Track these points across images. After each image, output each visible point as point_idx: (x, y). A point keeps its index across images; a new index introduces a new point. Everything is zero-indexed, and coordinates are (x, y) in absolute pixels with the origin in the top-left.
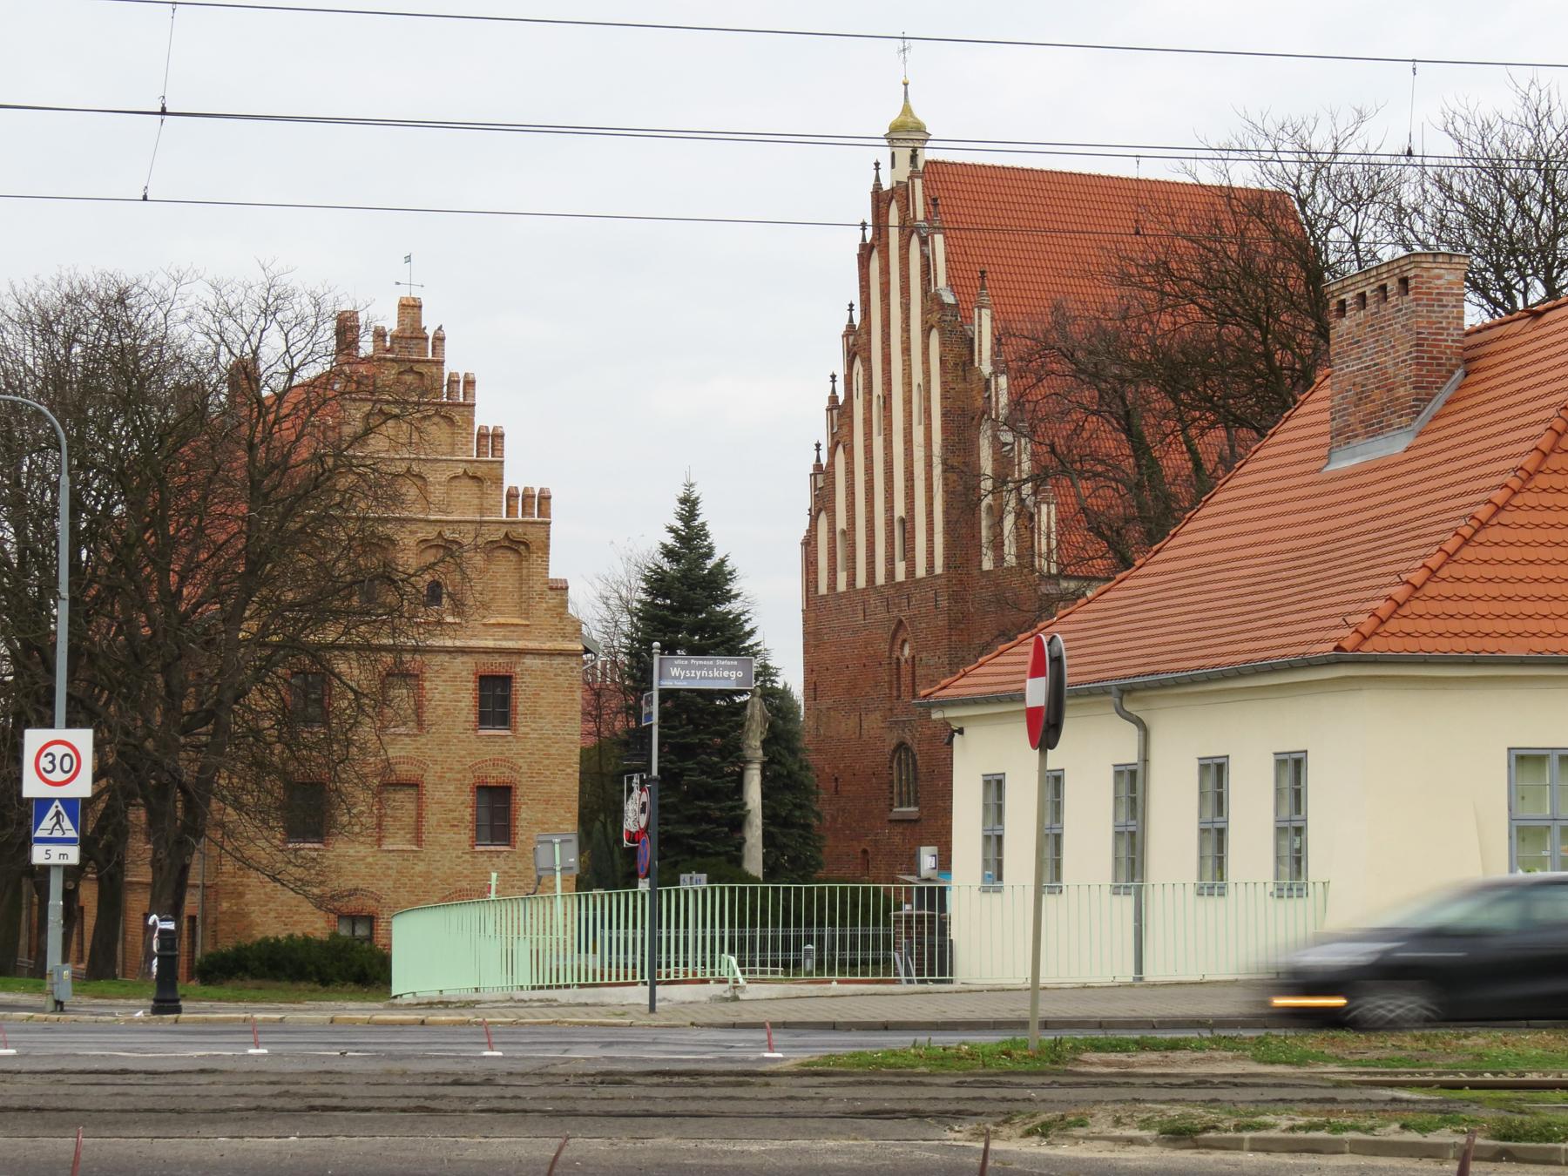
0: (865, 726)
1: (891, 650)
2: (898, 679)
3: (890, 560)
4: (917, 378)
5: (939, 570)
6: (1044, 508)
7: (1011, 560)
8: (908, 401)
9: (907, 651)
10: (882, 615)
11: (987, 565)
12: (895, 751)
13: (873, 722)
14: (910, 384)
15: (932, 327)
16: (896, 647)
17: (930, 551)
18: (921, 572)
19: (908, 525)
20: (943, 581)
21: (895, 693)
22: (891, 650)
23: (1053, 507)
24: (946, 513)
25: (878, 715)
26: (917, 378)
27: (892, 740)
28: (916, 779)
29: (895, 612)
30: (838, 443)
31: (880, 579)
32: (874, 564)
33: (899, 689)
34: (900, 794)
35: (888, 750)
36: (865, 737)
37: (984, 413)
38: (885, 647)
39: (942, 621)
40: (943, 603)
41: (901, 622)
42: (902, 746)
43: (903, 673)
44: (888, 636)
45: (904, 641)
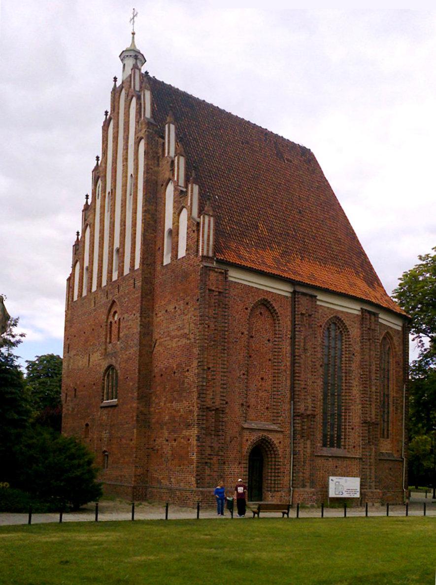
0: (91, 360)
1: (108, 318)
2: (111, 333)
3: (110, 272)
4: (131, 171)
5: (137, 266)
6: (207, 218)
7: (182, 253)
8: (125, 185)
9: (116, 318)
10: (104, 300)
11: (167, 260)
12: (105, 373)
13: (96, 357)
14: (126, 177)
15: (141, 138)
16: (111, 317)
17: (133, 258)
18: (126, 271)
19: (121, 250)
20: (140, 272)
21: (108, 340)
22: (108, 318)
23: (212, 219)
24: (144, 235)
25: (98, 354)
26: (131, 171)
27: (105, 364)
28: (117, 384)
29: (110, 297)
30: (87, 225)
31: (104, 283)
32: (104, 274)
33: (110, 338)
34: (108, 393)
35: (103, 370)
36: (91, 366)
37: (170, 180)
38: (104, 317)
39: (138, 294)
40: (139, 284)
41: (114, 302)
42: (110, 367)
43: (113, 328)
44: (106, 312)
45: (115, 312)
